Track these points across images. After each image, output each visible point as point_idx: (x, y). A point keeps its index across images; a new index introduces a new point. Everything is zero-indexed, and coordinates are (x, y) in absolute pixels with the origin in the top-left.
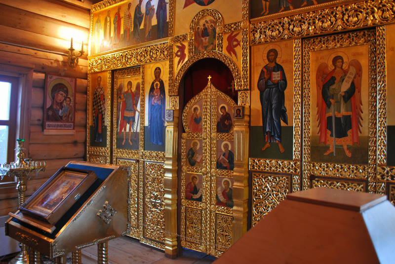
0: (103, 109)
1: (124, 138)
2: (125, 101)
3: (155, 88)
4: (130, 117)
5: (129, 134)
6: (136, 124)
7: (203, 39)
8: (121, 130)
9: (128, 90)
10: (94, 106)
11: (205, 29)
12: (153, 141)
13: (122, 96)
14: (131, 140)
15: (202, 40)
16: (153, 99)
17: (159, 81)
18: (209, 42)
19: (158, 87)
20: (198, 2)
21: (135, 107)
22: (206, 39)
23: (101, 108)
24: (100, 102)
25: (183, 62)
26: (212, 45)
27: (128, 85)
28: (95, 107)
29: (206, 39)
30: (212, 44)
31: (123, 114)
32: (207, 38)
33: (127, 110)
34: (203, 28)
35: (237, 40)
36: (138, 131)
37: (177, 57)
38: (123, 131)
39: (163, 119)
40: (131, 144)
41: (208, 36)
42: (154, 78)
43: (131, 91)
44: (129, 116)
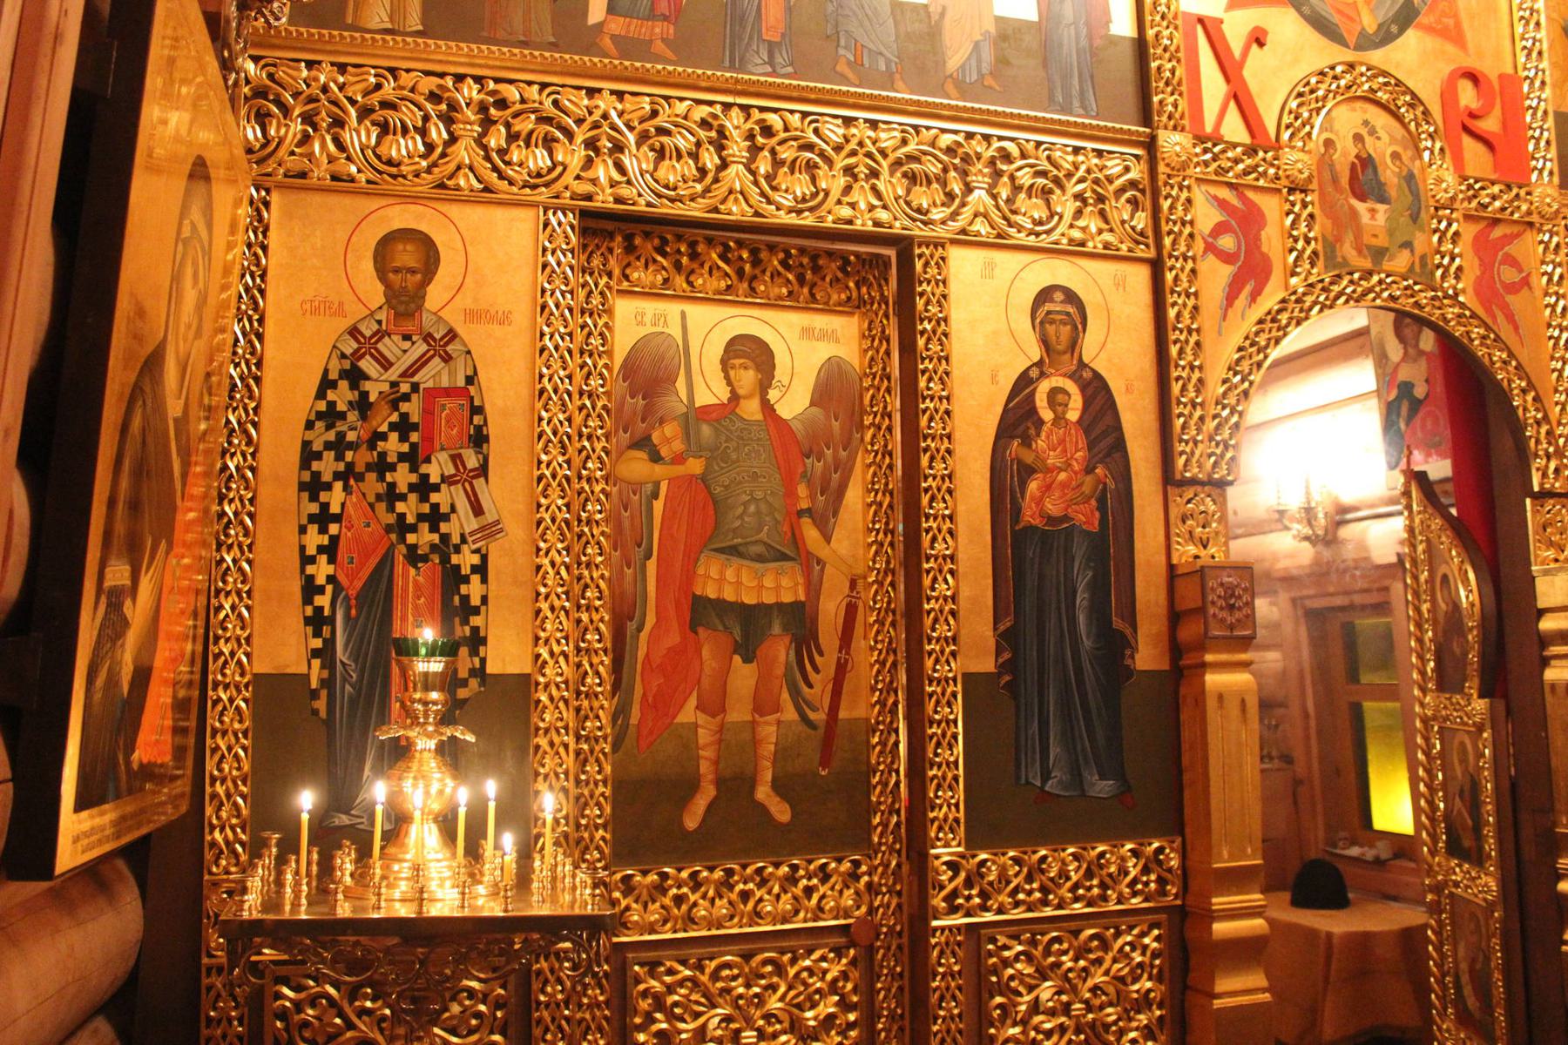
0: (462, 522)
1: (705, 767)
2: (704, 479)
3: (1047, 415)
4: (760, 607)
5: (755, 742)
6: (828, 662)
7: (1361, 207)
8: (662, 705)
9: (735, 397)
10: (314, 487)
11: (1365, 163)
12: (1046, 776)
13: (668, 436)
14: (778, 786)
15: (1354, 213)
16: (1033, 486)
17: (1071, 377)
18: (1391, 232)
19: (1073, 415)
20: (1306, 10)
21: (811, 533)
22: (1373, 211)
23: (435, 518)
24: (413, 458)
25: (1254, 297)
26: (1406, 253)
27: (725, 364)
28: (335, 498)
29: (1373, 211)
30: (1408, 245)
31: (689, 576)
32: (1381, 208)
33: (734, 551)
34: (1354, 151)
35: (1512, 262)
36: (858, 707)
37: (1211, 257)
38: (688, 713)
39: (1117, 623)
40: (781, 812)
41: (1383, 199)
42: (1036, 353)
43: (768, 408)
44: (749, 599)
